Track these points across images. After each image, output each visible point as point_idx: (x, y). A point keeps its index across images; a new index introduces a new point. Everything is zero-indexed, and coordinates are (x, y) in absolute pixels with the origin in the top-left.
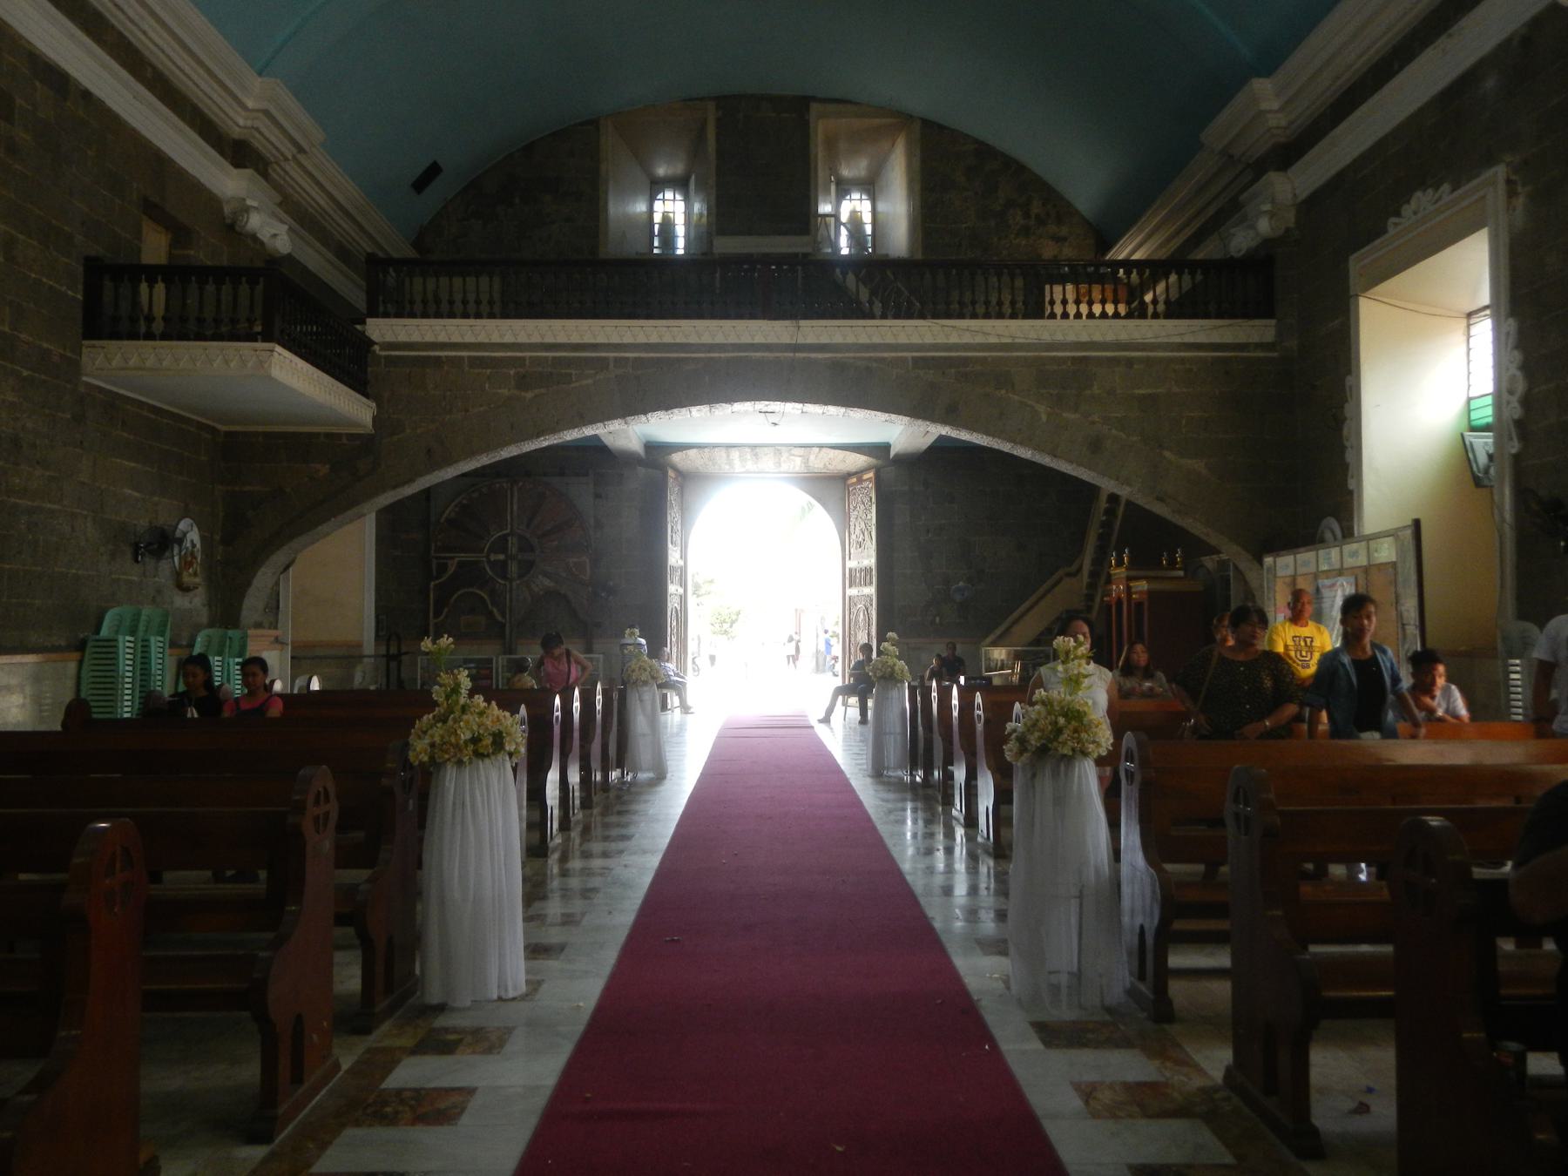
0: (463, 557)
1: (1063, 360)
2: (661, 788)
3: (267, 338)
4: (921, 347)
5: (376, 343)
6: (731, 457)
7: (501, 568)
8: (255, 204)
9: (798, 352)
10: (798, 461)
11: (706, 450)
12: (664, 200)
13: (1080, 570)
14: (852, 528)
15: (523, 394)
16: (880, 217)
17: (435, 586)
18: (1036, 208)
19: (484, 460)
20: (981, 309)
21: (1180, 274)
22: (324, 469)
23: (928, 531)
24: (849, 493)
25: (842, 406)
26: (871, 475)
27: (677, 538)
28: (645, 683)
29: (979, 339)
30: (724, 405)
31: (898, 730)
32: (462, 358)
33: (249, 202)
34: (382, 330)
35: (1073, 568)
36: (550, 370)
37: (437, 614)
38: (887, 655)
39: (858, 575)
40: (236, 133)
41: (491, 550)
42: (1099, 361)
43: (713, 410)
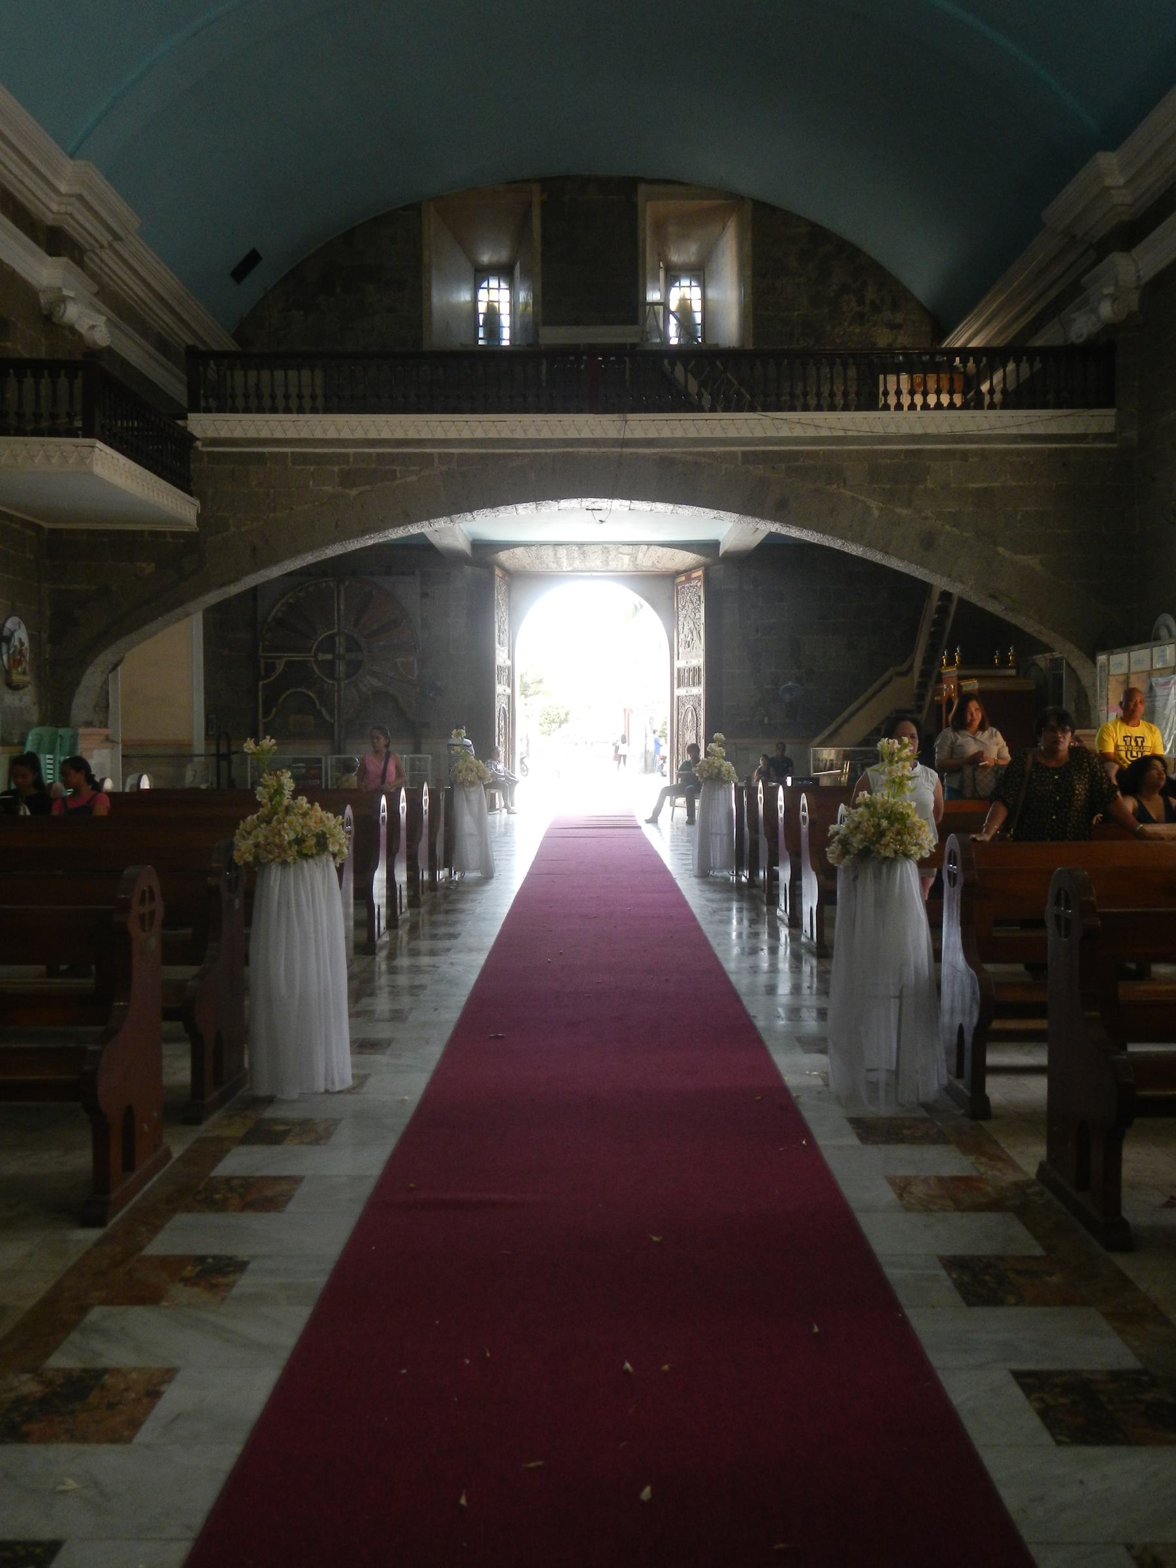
1: (897, 453)
2: (488, 888)
3: (88, 433)
5: (194, 439)
6: (558, 556)
7: (329, 668)
8: (72, 294)
9: (625, 447)
10: (626, 559)
11: (533, 548)
12: (488, 289)
13: (911, 668)
14: (681, 627)
15: (347, 491)
16: (710, 304)
17: (265, 686)
18: (871, 294)
19: (309, 559)
20: (812, 401)
21: (1018, 363)
22: (149, 568)
23: (757, 631)
24: (677, 593)
25: (671, 503)
26: (700, 573)
27: (505, 638)
28: (472, 784)
29: (811, 432)
30: (550, 501)
31: (725, 830)
32: (285, 455)
33: (66, 292)
34: (203, 425)
35: (904, 667)
36: (373, 466)
37: (266, 713)
38: (714, 755)
39: (686, 674)
40: (50, 220)
43: (539, 507)
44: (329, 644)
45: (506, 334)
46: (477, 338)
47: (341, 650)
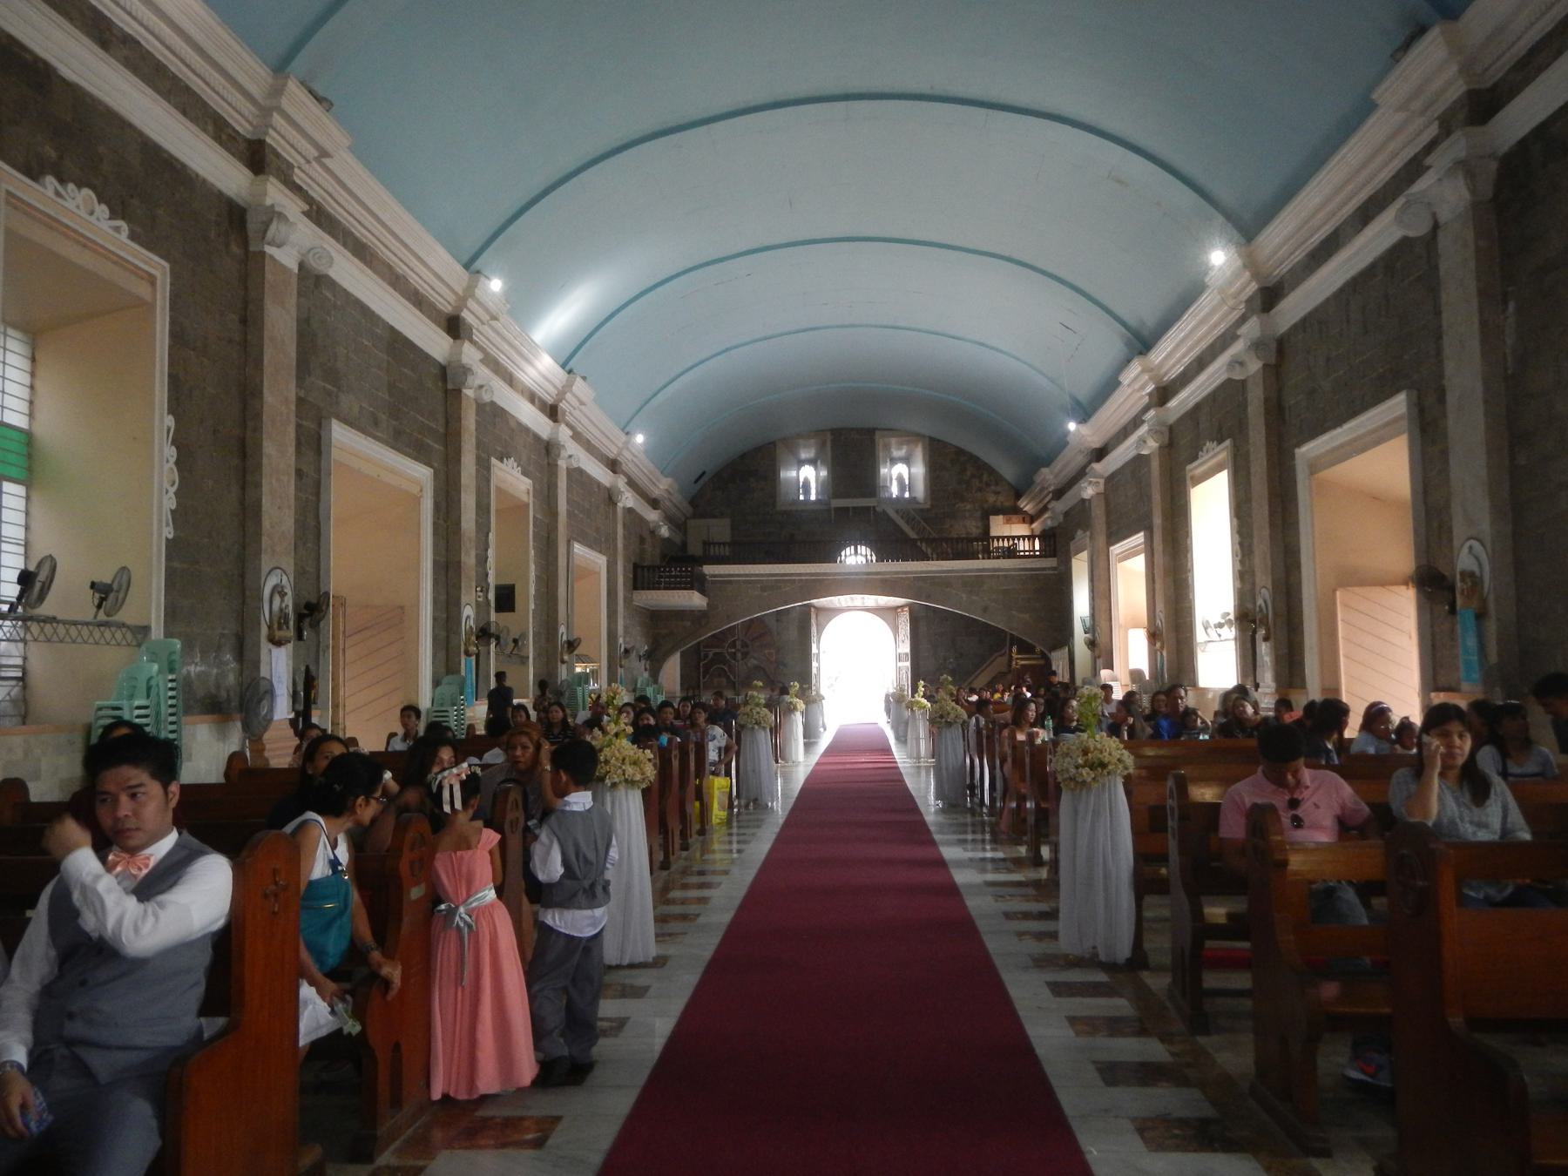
0: (717, 650)
3: (692, 588)
4: (916, 572)
7: (734, 655)
18: (985, 477)
22: (689, 624)
26: (906, 609)
29: (940, 569)
34: (709, 570)
40: (654, 496)
44: (733, 645)
47: (739, 647)
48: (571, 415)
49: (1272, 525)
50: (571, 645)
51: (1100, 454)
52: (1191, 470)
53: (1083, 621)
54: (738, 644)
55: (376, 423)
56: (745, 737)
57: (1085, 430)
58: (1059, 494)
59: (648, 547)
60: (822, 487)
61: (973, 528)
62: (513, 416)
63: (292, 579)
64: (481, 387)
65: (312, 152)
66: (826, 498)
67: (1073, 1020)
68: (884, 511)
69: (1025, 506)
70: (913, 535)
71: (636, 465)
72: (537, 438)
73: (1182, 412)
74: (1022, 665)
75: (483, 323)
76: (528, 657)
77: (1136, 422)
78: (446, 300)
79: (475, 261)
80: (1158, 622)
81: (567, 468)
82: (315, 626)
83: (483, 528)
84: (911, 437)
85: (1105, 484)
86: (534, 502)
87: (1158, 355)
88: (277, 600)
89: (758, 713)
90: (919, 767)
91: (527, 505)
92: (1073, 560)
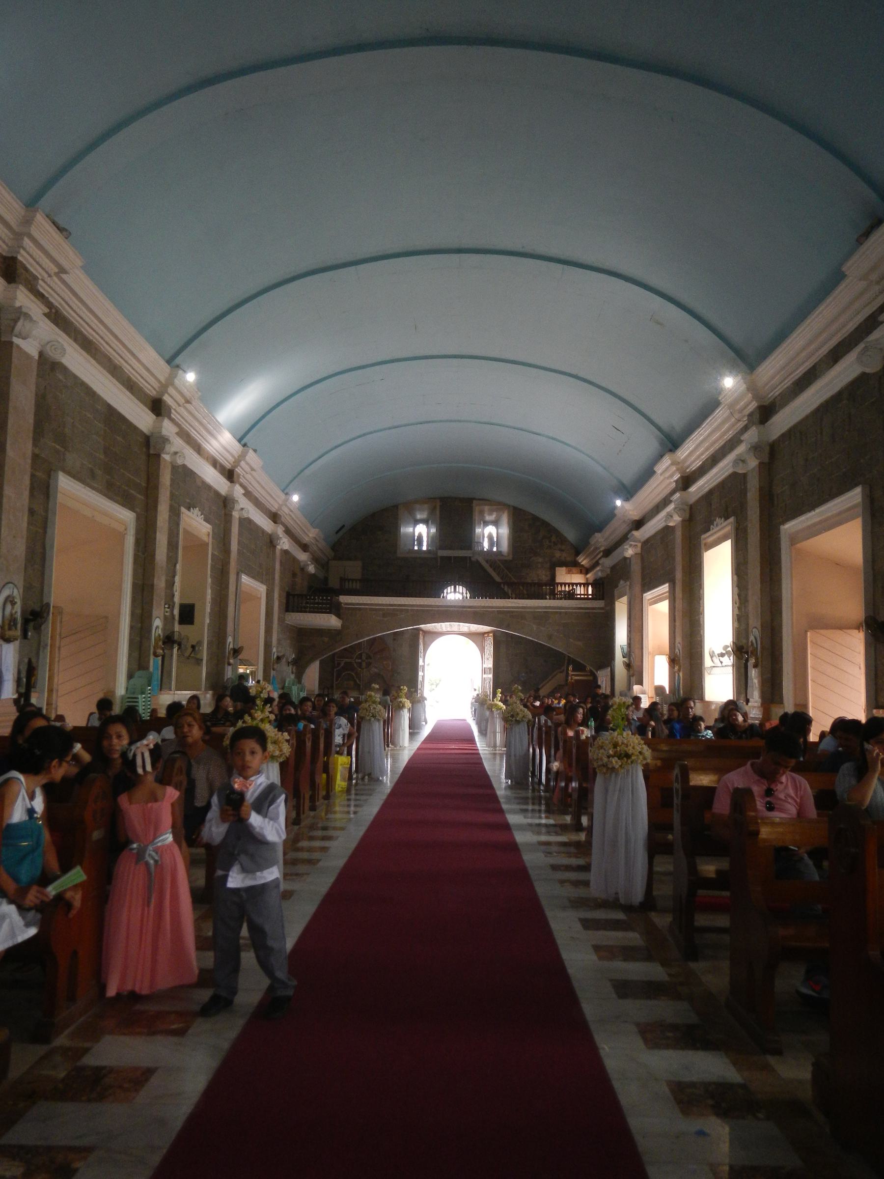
5: (342, 603)
7: (360, 665)
13: (564, 670)
18: (554, 539)
26: (492, 635)
27: (422, 655)
29: (517, 605)
32: (367, 608)
34: (344, 599)
40: (305, 542)
41: (357, 658)
42: (552, 613)
44: (361, 655)
45: (425, 544)
46: (414, 545)
48: (244, 477)
49: (762, 581)
50: (236, 652)
51: (639, 524)
52: (705, 539)
53: (622, 648)
54: (364, 657)
55: (93, 476)
56: (364, 726)
57: (628, 506)
58: (607, 553)
59: (298, 580)
60: (432, 540)
61: (544, 576)
62: (200, 477)
63: (21, 591)
64: (176, 453)
65: (54, 269)
66: (435, 549)
67: (597, 948)
68: (478, 561)
69: (583, 561)
70: (498, 579)
71: (293, 519)
72: (217, 494)
73: (700, 495)
74: (576, 680)
75: (179, 405)
76: (202, 660)
77: (666, 502)
78: (151, 386)
79: (175, 358)
80: (677, 650)
81: (240, 519)
82: (38, 628)
83: (172, 560)
84: (499, 506)
85: (642, 548)
86: (212, 542)
87: (683, 453)
88: (9, 607)
89: (374, 708)
90: (495, 754)
91: (207, 544)
92: (617, 603)
